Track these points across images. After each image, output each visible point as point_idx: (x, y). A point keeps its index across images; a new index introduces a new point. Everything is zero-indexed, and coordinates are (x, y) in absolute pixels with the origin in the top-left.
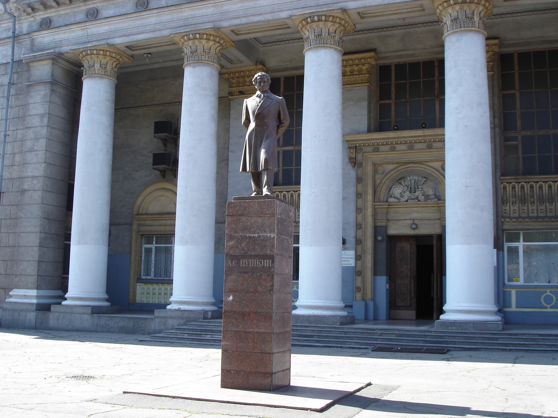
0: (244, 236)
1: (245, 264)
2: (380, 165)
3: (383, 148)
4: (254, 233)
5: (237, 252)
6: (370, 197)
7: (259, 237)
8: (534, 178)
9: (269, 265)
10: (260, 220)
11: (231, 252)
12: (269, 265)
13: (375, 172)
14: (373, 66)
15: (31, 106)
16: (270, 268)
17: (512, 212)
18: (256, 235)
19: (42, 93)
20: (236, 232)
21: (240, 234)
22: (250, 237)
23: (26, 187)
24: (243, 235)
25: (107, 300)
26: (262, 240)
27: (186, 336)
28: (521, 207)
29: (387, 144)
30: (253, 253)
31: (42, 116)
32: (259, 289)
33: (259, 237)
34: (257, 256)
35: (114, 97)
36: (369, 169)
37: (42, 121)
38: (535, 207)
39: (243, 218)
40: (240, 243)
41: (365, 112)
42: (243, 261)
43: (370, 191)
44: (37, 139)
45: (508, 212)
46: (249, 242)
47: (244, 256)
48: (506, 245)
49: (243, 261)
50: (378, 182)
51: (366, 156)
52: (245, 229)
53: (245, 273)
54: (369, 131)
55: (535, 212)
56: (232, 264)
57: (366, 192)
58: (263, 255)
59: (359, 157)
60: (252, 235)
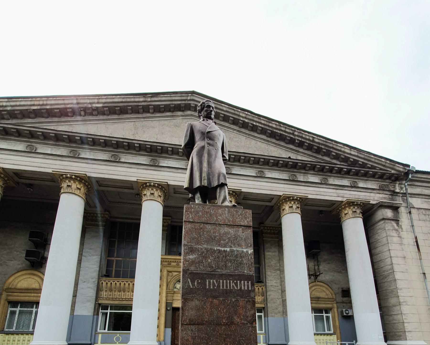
0: (211, 249)
1: (214, 285)
3: (173, 264)
4: (225, 247)
5: (201, 269)
7: (232, 251)
9: (248, 287)
10: (232, 231)
11: (192, 268)
12: (248, 287)
13: (168, 275)
16: (249, 292)
18: (228, 249)
20: (198, 243)
21: (205, 246)
22: (220, 251)
24: (209, 247)
26: (236, 256)
29: (175, 262)
30: (224, 272)
32: (236, 319)
33: (232, 251)
34: (231, 275)
39: (209, 227)
40: (206, 258)
42: (209, 282)
46: (218, 257)
47: (211, 276)
49: (209, 282)
52: (211, 240)
53: (215, 297)
56: (194, 285)
58: (239, 275)
60: (223, 249)
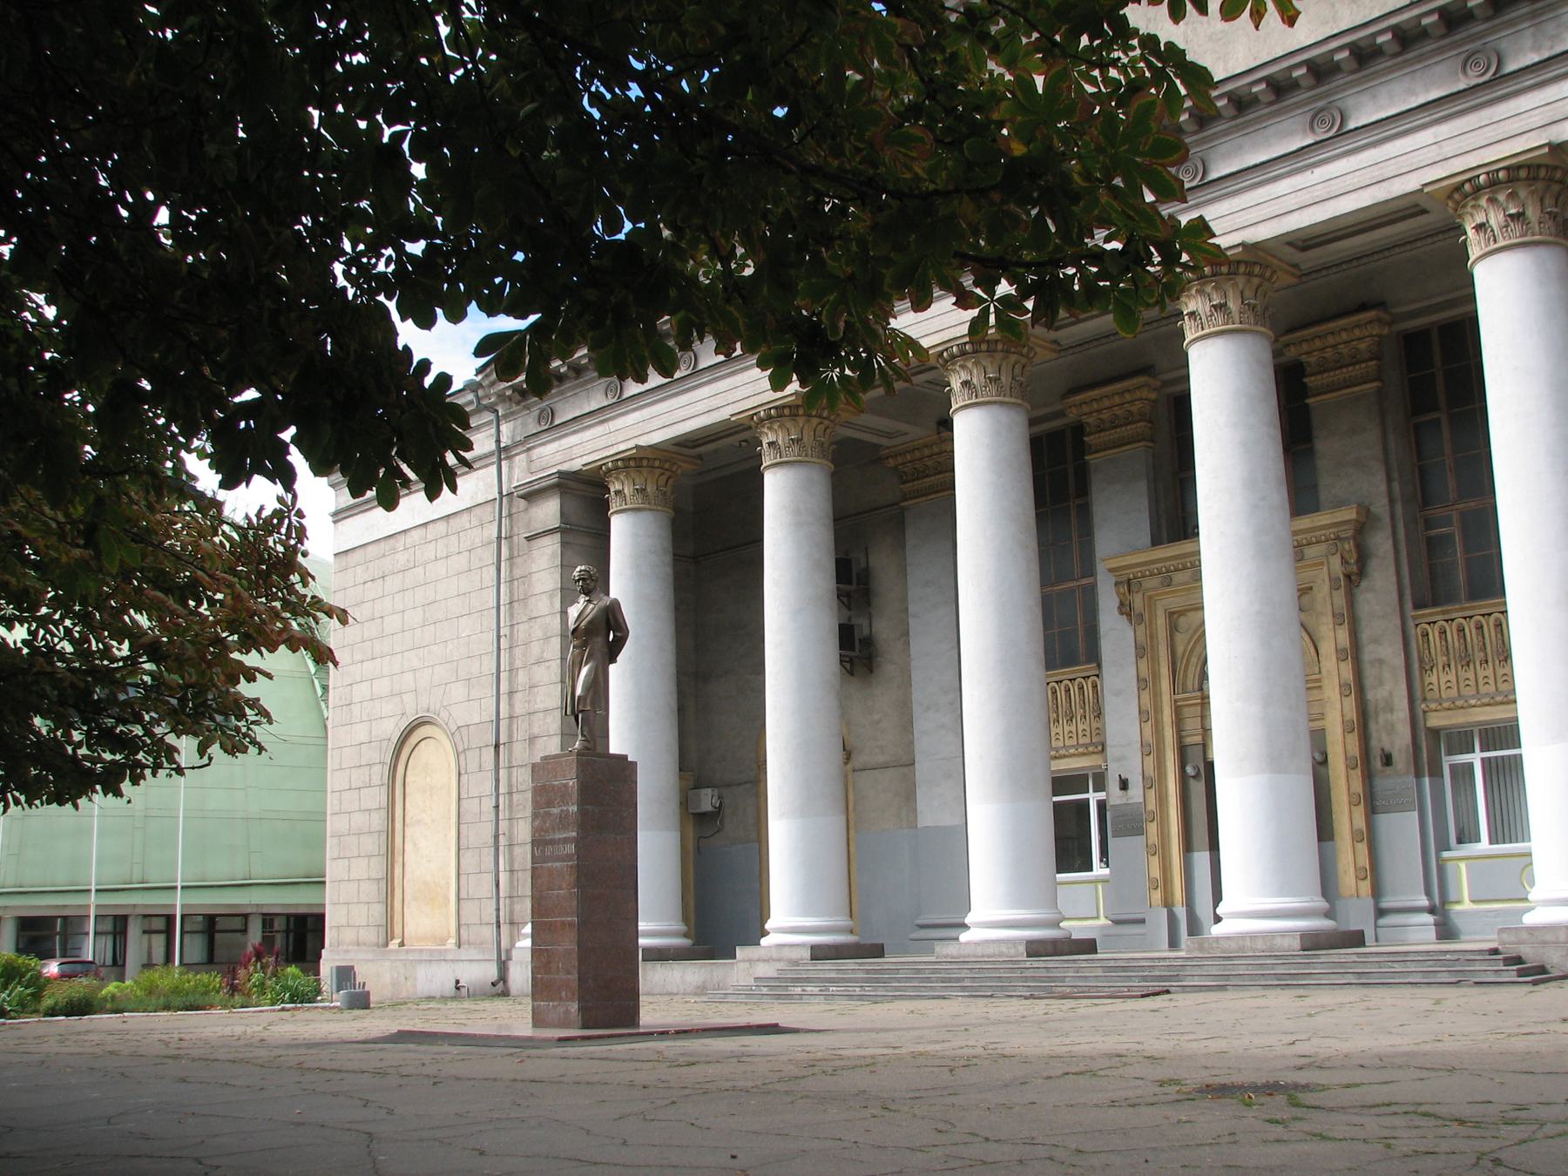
2: (1182, 613)
6: (1165, 685)
8: (1480, 607)
14: (1154, 402)
15: (535, 577)
17: (1443, 687)
19: (549, 550)
23: (536, 731)
25: (685, 935)
27: (765, 991)
28: (1462, 674)
29: (1185, 568)
31: (551, 595)
35: (668, 544)
36: (1161, 622)
37: (552, 604)
38: (1489, 672)
41: (1143, 504)
43: (1165, 671)
44: (547, 639)
45: (1435, 688)
48: (1447, 761)
50: (1180, 649)
51: (1150, 598)
54: (1156, 541)
55: (1491, 681)
57: (1156, 676)
59: (1138, 601)
